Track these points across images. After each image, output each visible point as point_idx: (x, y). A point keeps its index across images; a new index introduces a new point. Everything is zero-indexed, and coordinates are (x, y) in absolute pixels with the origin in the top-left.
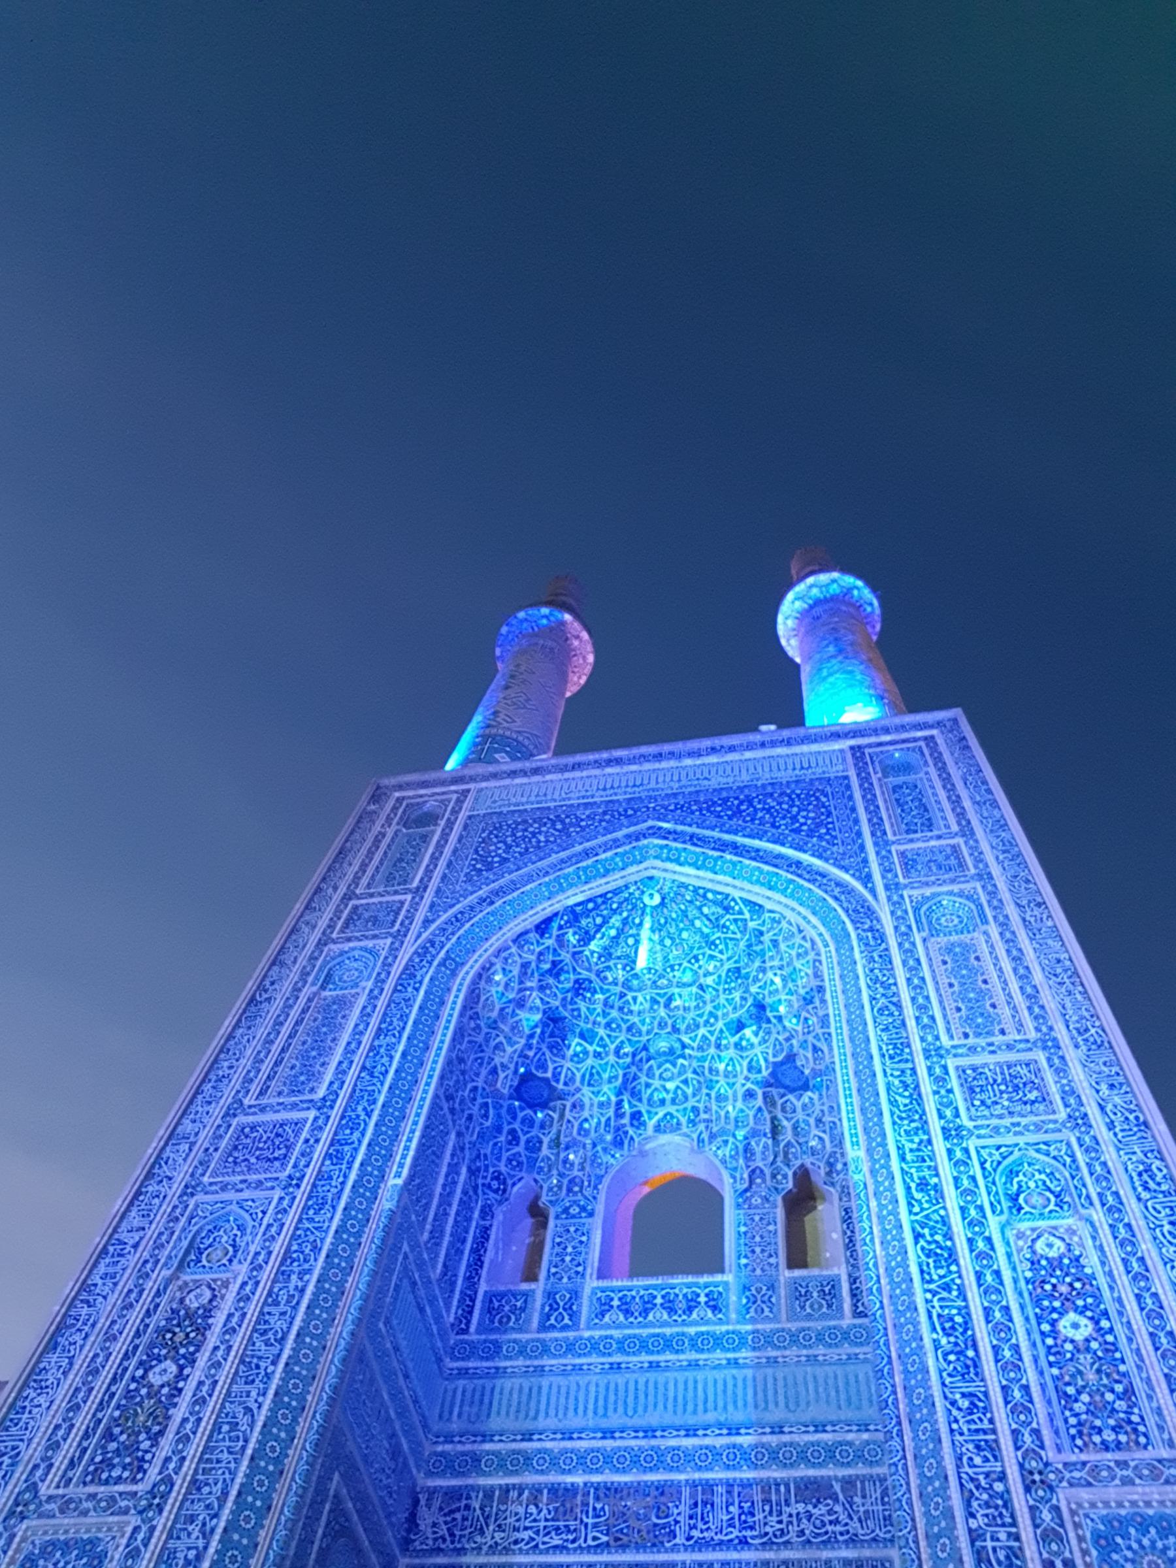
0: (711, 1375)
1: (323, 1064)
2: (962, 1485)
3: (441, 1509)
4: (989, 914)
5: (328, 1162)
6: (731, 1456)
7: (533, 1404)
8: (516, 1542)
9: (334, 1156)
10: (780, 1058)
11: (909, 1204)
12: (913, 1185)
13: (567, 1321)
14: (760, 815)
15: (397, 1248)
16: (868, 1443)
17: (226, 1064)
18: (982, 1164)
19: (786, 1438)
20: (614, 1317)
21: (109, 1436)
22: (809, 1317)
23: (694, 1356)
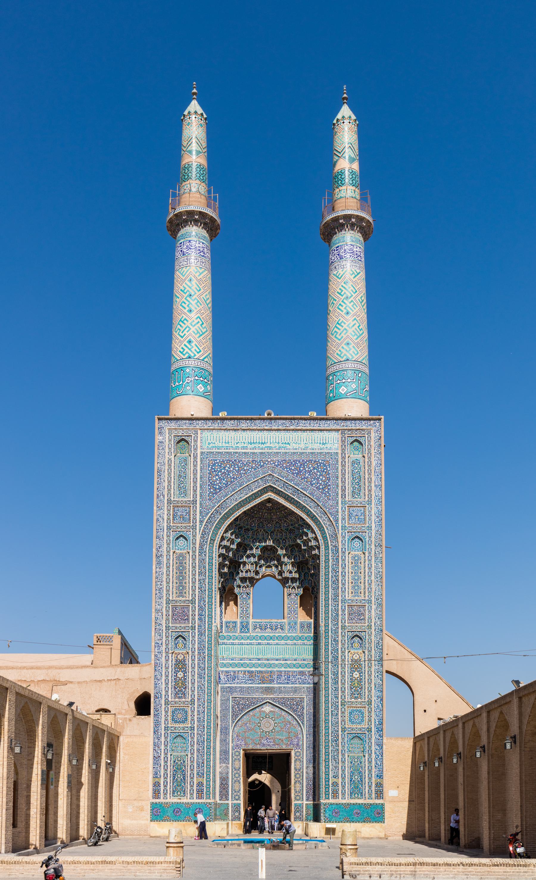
4: (367, 547)
17: (159, 583)
21: (175, 688)
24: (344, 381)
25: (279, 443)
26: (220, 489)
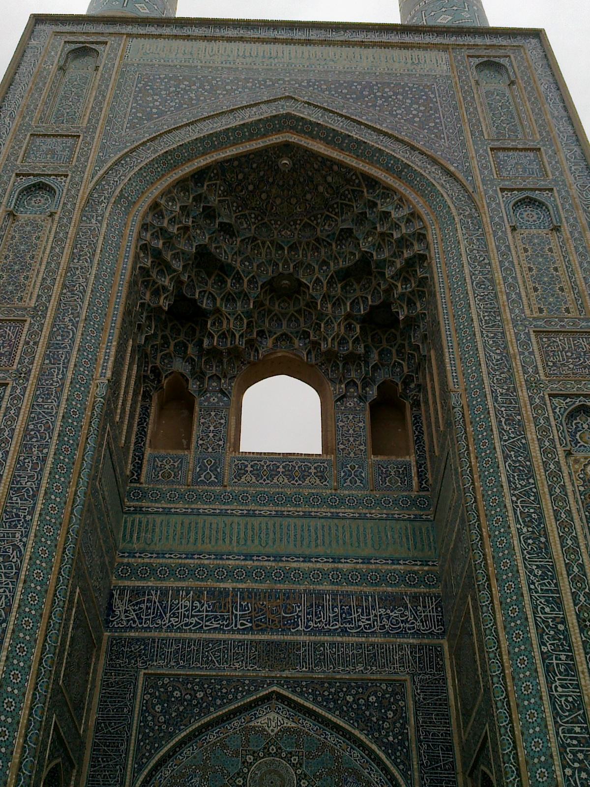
0: (319, 523)
1: (27, 278)
2: (537, 624)
3: (130, 601)
5: (47, 361)
6: (335, 576)
7: (192, 535)
8: (186, 625)
9: (51, 356)
10: (377, 303)
11: (500, 432)
12: (503, 420)
13: (213, 479)
14: (380, 102)
15: (104, 429)
16: (428, 572)
18: (554, 410)
19: (373, 567)
20: (249, 479)
22: (389, 488)
23: (308, 509)
24: (443, 10)
25: (309, 58)
26: (161, 114)
